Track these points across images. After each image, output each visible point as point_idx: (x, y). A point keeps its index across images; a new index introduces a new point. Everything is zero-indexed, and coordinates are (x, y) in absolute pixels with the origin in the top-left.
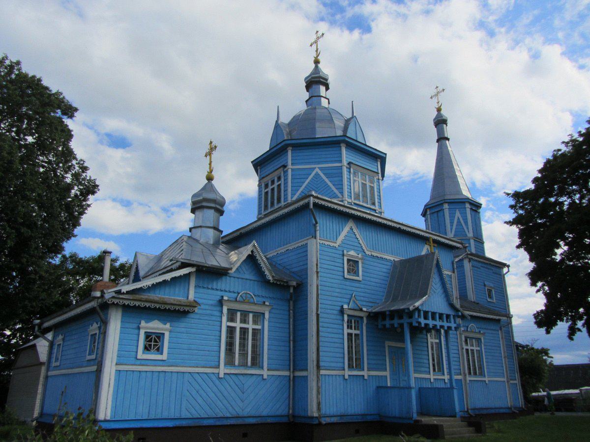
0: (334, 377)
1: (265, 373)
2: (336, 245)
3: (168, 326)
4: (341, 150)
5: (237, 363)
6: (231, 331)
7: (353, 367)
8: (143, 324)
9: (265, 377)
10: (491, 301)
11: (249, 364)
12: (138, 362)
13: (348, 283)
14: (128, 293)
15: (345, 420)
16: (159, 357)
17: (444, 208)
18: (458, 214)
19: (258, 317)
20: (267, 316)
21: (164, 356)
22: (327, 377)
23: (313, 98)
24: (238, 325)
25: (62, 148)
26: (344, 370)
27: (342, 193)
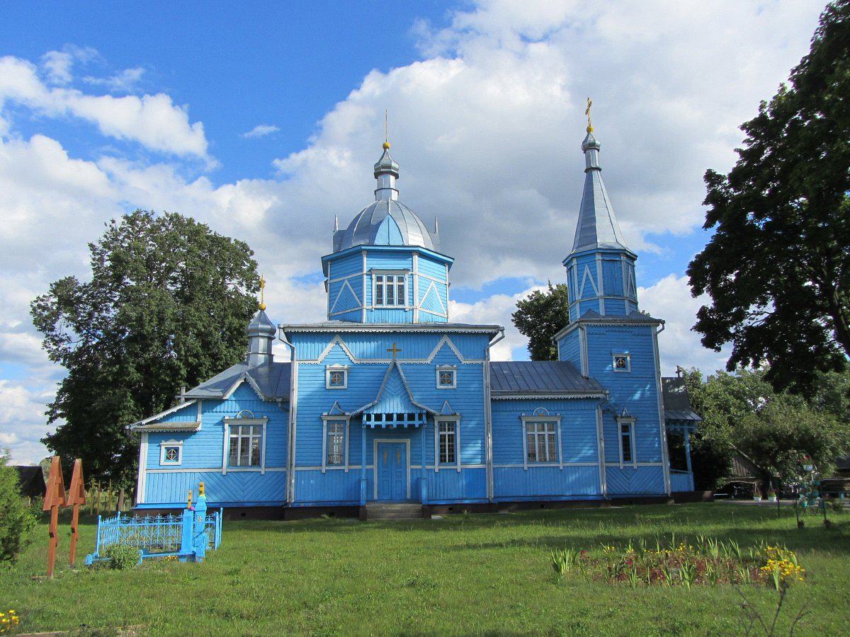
0: (534, 469)
1: (263, 470)
2: (318, 362)
3: (181, 442)
4: (362, 259)
5: (239, 463)
6: (234, 441)
7: (445, 461)
8: (163, 443)
9: (459, 470)
10: (625, 371)
11: (250, 463)
12: (161, 467)
13: (331, 393)
14: (147, 424)
15: (321, 505)
16: (176, 463)
17: (596, 259)
18: (587, 270)
19: (258, 429)
20: (265, 427)
21: (180, 462)
22: (303, 472)
23: (383, 191)
24: (240, 436)
25: (97, 343)
26: (321, 466)
27: (362, 302)
